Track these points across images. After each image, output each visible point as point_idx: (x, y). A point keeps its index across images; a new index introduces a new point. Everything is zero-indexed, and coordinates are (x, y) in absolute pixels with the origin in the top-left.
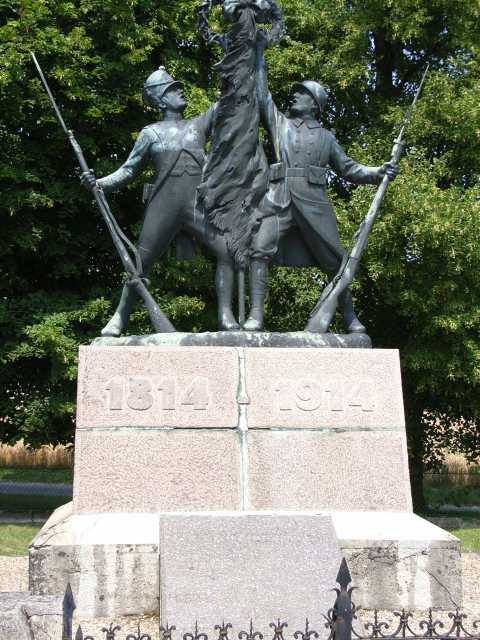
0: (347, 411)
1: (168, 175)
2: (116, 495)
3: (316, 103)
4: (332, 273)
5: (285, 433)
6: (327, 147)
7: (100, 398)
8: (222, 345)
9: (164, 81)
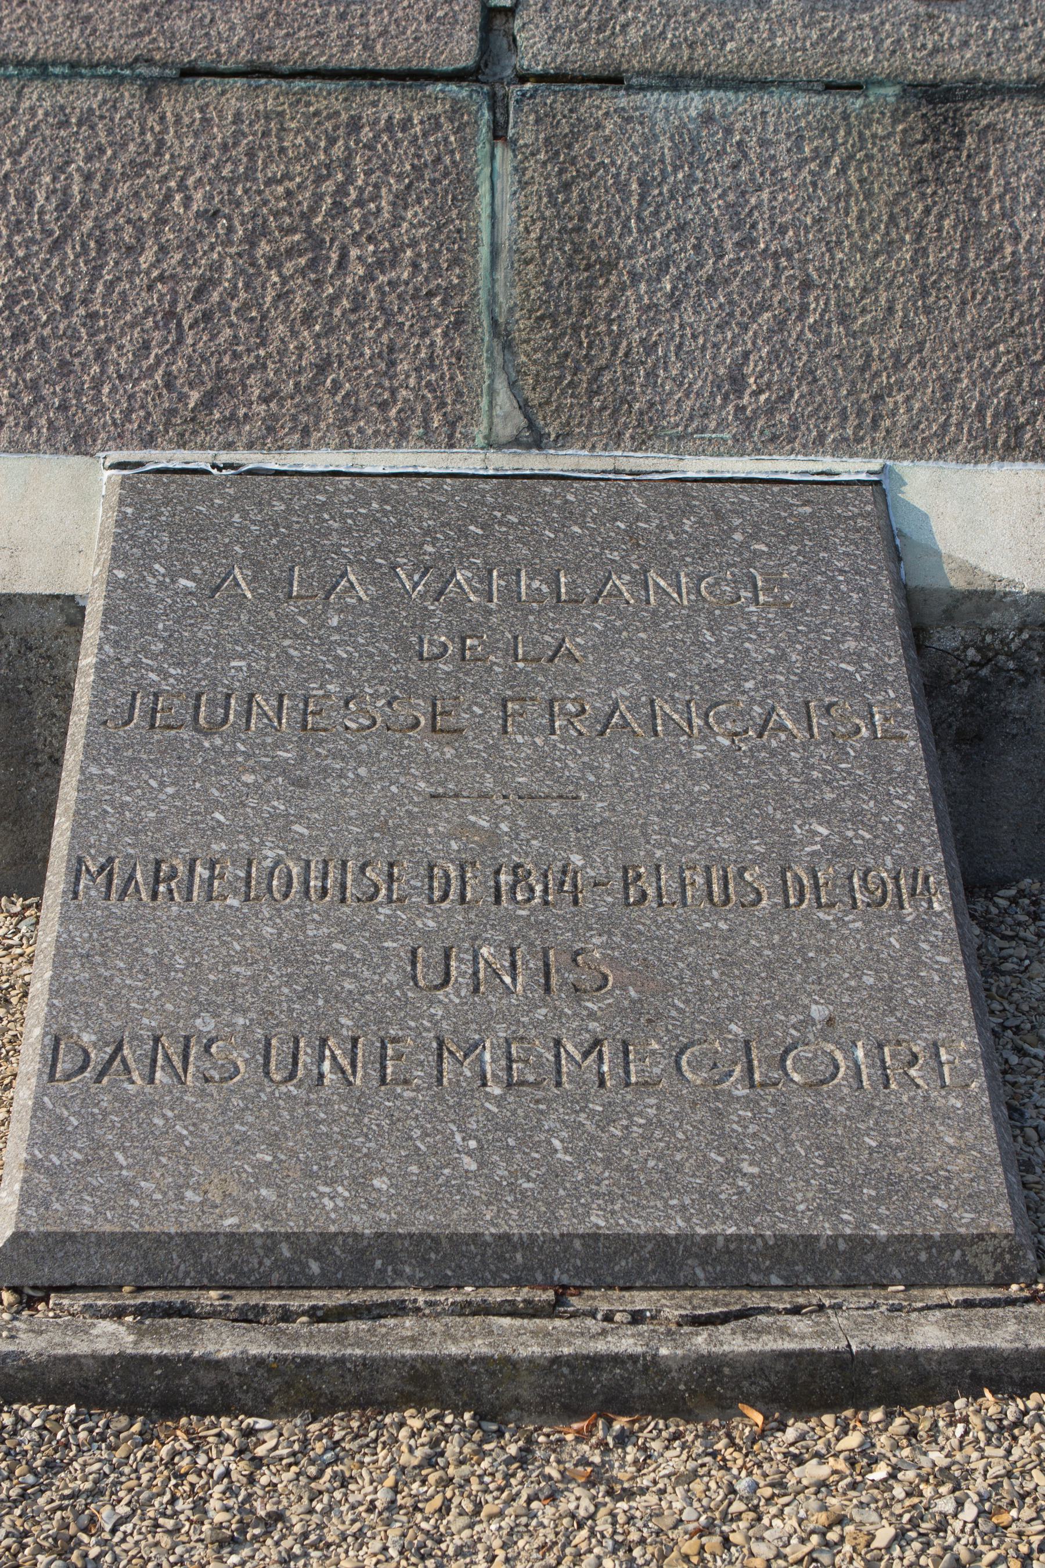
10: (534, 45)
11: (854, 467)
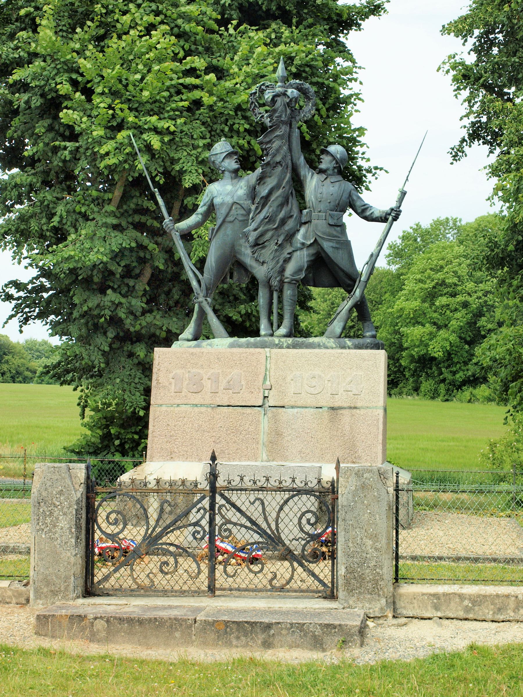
0: (342, 394)
1: (224, 221)
2: (176, 450)
3: (337, 163)
4: (349, 289)
5: (296, 410)
6: (346, 195)
7: (167, 384)
8: (257, 347)
10: (271, 402)
11: (319, 465)
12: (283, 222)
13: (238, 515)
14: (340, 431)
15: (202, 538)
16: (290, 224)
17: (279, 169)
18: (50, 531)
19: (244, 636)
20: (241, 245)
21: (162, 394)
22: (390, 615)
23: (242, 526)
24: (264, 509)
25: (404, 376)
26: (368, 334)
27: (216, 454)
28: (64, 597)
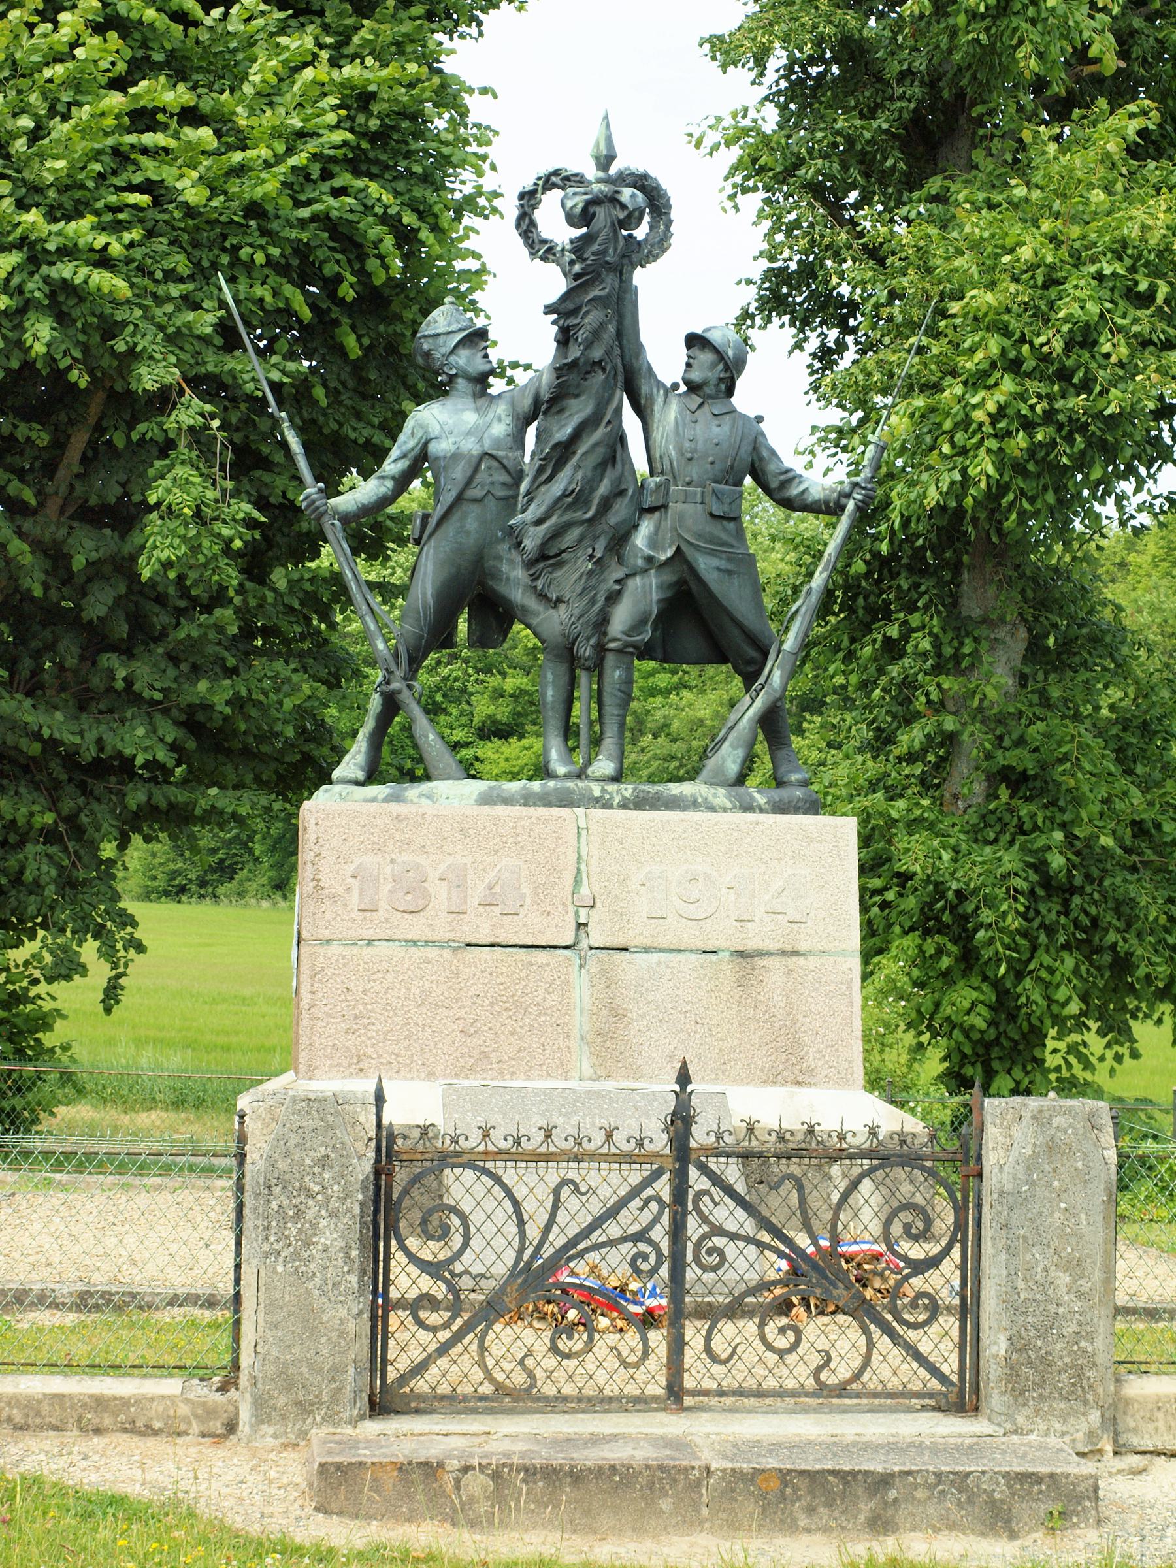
1: (459, 499)
2: (370, 1051)
5: (655, 957)
6: (746, 448)
7: (341, 891)
8: (549, 804)
9: (454, 327)
11: (718, 1088)
12: (606, 505)
13: (741, 1214)
14: (763, 1007)
15: (654, 1270)
16: (620, 512)
17: (599, 377)
18: (296, 1255)
19: (826, 1505)
20: (499, 558)
21: (329, 915)
22: (1109, 1448)
23: (749, 1240)
24: (803, 1201)
25: (251, 852)
26: (794, 777)
27: (691, 1069)
28: (328, 1419)
